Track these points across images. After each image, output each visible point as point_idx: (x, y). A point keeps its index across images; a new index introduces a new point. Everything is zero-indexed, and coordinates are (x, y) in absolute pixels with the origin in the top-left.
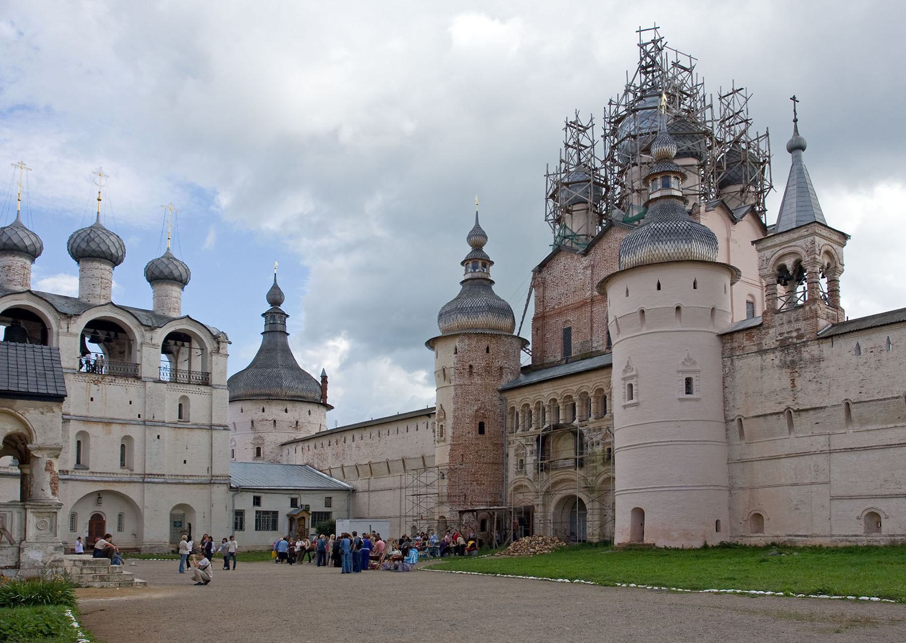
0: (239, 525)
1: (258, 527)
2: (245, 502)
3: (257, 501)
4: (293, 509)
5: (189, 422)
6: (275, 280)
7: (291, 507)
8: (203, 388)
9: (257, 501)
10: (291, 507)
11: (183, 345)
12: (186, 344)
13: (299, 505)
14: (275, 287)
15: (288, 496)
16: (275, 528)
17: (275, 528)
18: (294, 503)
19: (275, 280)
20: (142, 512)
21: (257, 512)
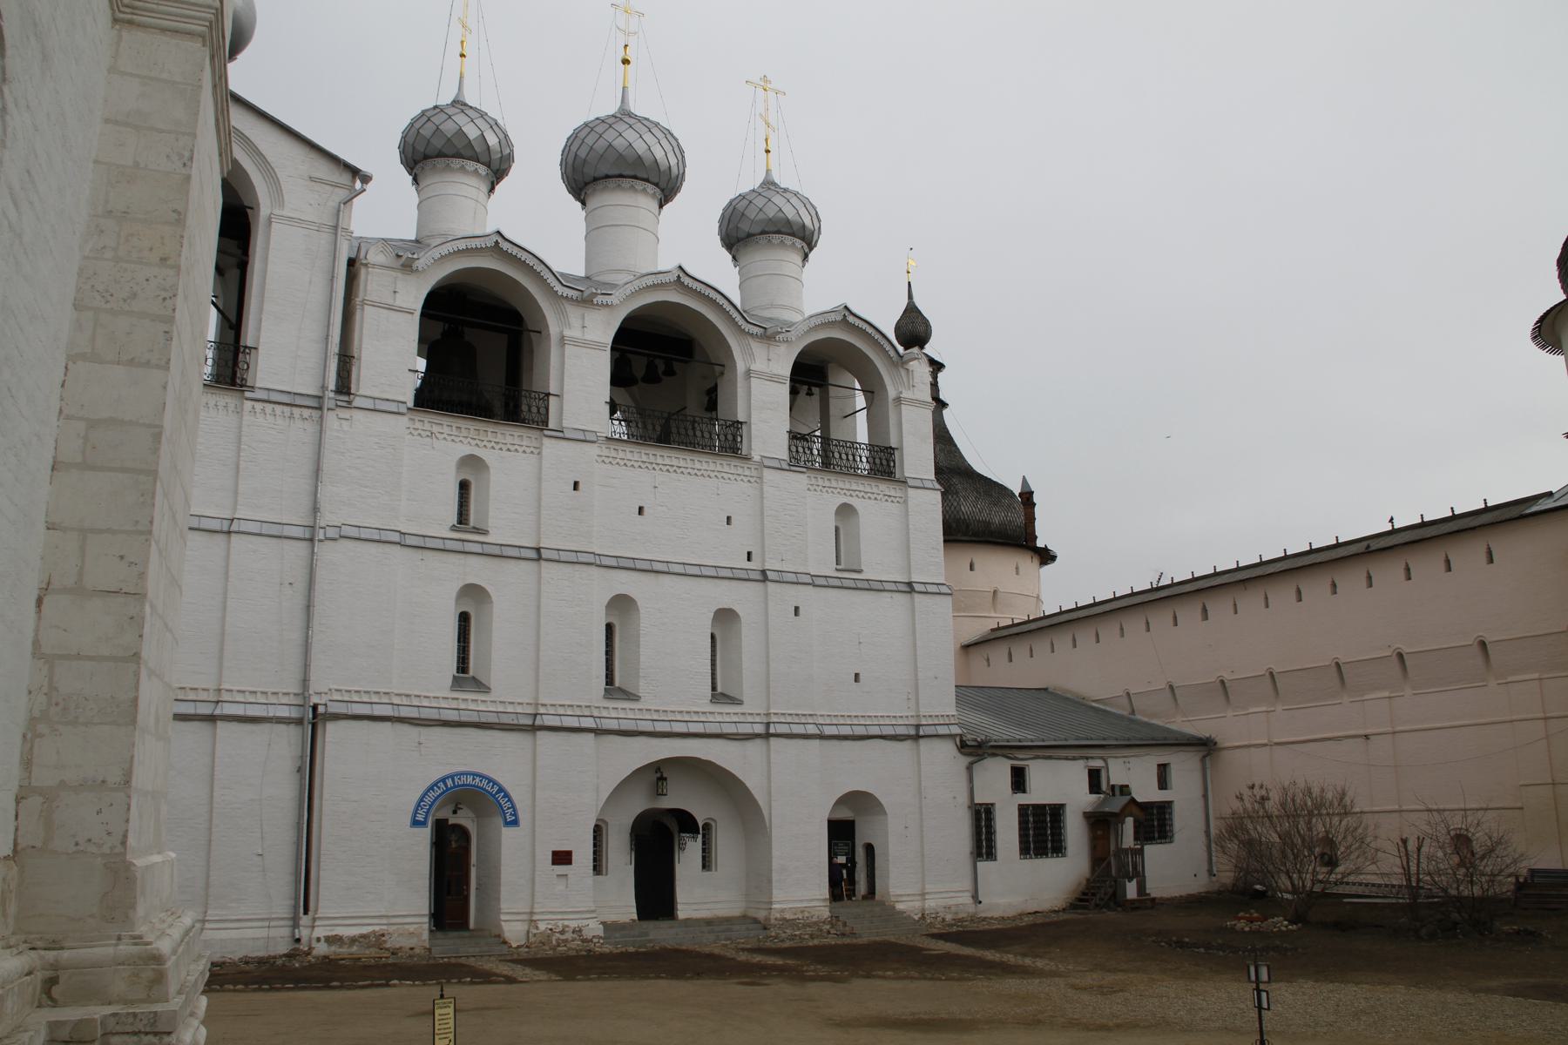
0: (984, 846)
1: (1025, 851)
2: (994, 779)
3: (1019, 780)
4: (1094, 796)
5: (860, 571)
6: (910, 296)
7: (1091, 793)
8: (884, 488)
9: (1019, 780)
10: (1091, 793)
11: (810, 394)
12: (816, 390)
13: (1104, 787)
14: (912, 311)
15: (1081, 763)
16: (1058, 849)
17: (1058, 849)
18: (1094, 778)
19: (910, 296)
20: (765, 813)
21: (1023, 809)
